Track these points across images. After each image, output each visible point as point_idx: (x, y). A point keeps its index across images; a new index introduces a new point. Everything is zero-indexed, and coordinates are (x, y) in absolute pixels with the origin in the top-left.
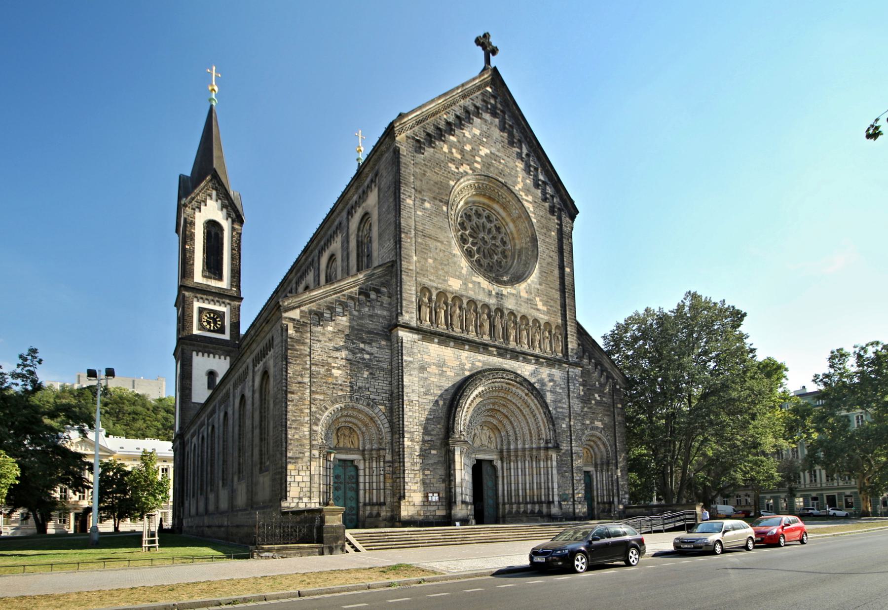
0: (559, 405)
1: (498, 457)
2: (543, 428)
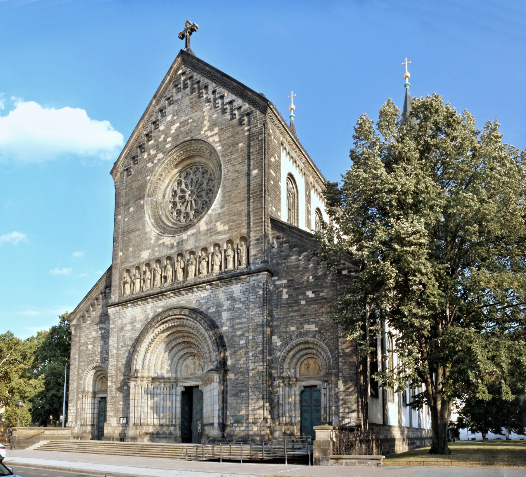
0: (237, 321)
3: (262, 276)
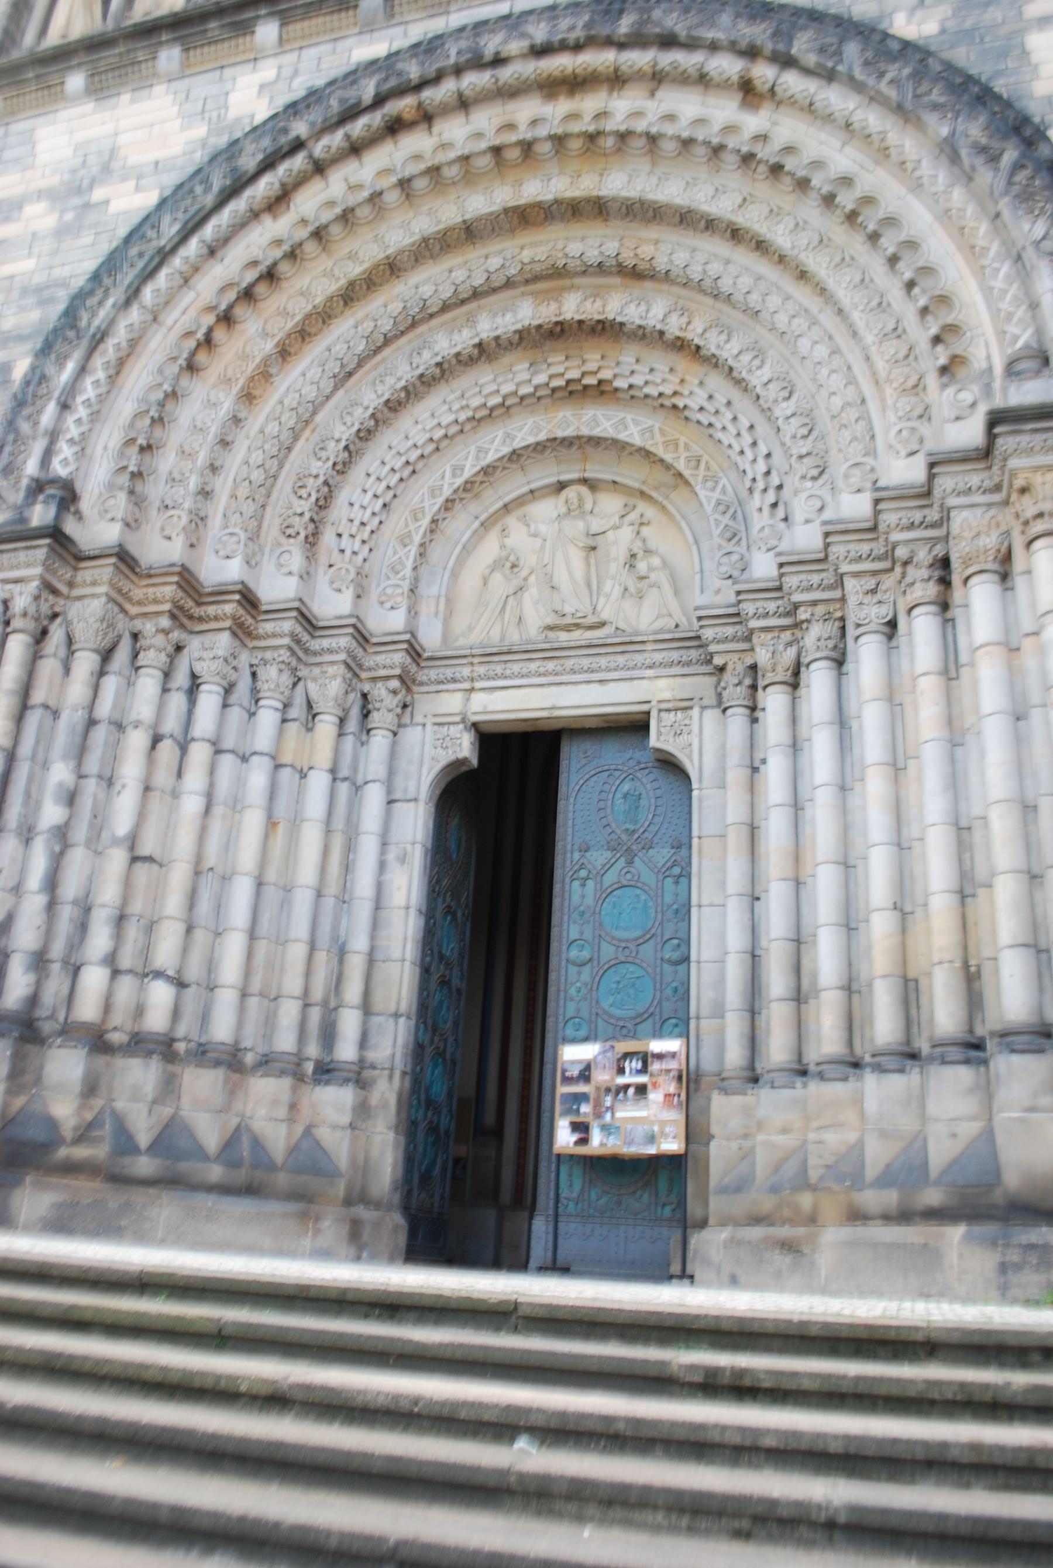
1: (702, 685)
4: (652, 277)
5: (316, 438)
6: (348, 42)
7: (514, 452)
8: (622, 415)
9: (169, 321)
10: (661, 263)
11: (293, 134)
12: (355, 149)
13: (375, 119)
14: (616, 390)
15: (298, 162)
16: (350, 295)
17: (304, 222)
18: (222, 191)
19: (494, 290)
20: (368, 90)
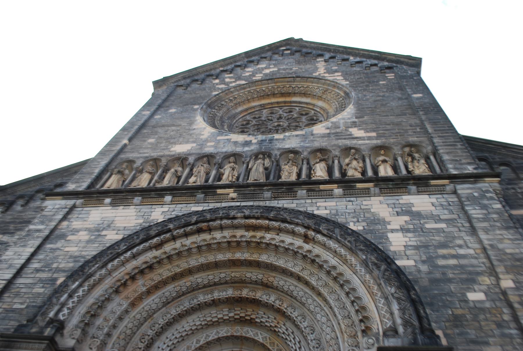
2: (371, 306)
3: (487, 185)
4: (272, 288)
5: (152, 322)
6: (191, 205)
7: (219, 338)
8: (257, 331)
9: (114, 275)
10: (275, 283)
11: (169, 227)
12: (186, 235)
13: (194, 227)
14: (256, 322)
15: (168, 235)
16: (175, 278)
17: (165, 253)
18: (142, 239)
19: (221, 284)
20: (194, 219)
